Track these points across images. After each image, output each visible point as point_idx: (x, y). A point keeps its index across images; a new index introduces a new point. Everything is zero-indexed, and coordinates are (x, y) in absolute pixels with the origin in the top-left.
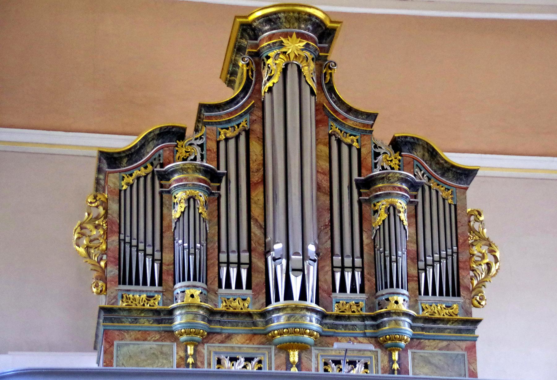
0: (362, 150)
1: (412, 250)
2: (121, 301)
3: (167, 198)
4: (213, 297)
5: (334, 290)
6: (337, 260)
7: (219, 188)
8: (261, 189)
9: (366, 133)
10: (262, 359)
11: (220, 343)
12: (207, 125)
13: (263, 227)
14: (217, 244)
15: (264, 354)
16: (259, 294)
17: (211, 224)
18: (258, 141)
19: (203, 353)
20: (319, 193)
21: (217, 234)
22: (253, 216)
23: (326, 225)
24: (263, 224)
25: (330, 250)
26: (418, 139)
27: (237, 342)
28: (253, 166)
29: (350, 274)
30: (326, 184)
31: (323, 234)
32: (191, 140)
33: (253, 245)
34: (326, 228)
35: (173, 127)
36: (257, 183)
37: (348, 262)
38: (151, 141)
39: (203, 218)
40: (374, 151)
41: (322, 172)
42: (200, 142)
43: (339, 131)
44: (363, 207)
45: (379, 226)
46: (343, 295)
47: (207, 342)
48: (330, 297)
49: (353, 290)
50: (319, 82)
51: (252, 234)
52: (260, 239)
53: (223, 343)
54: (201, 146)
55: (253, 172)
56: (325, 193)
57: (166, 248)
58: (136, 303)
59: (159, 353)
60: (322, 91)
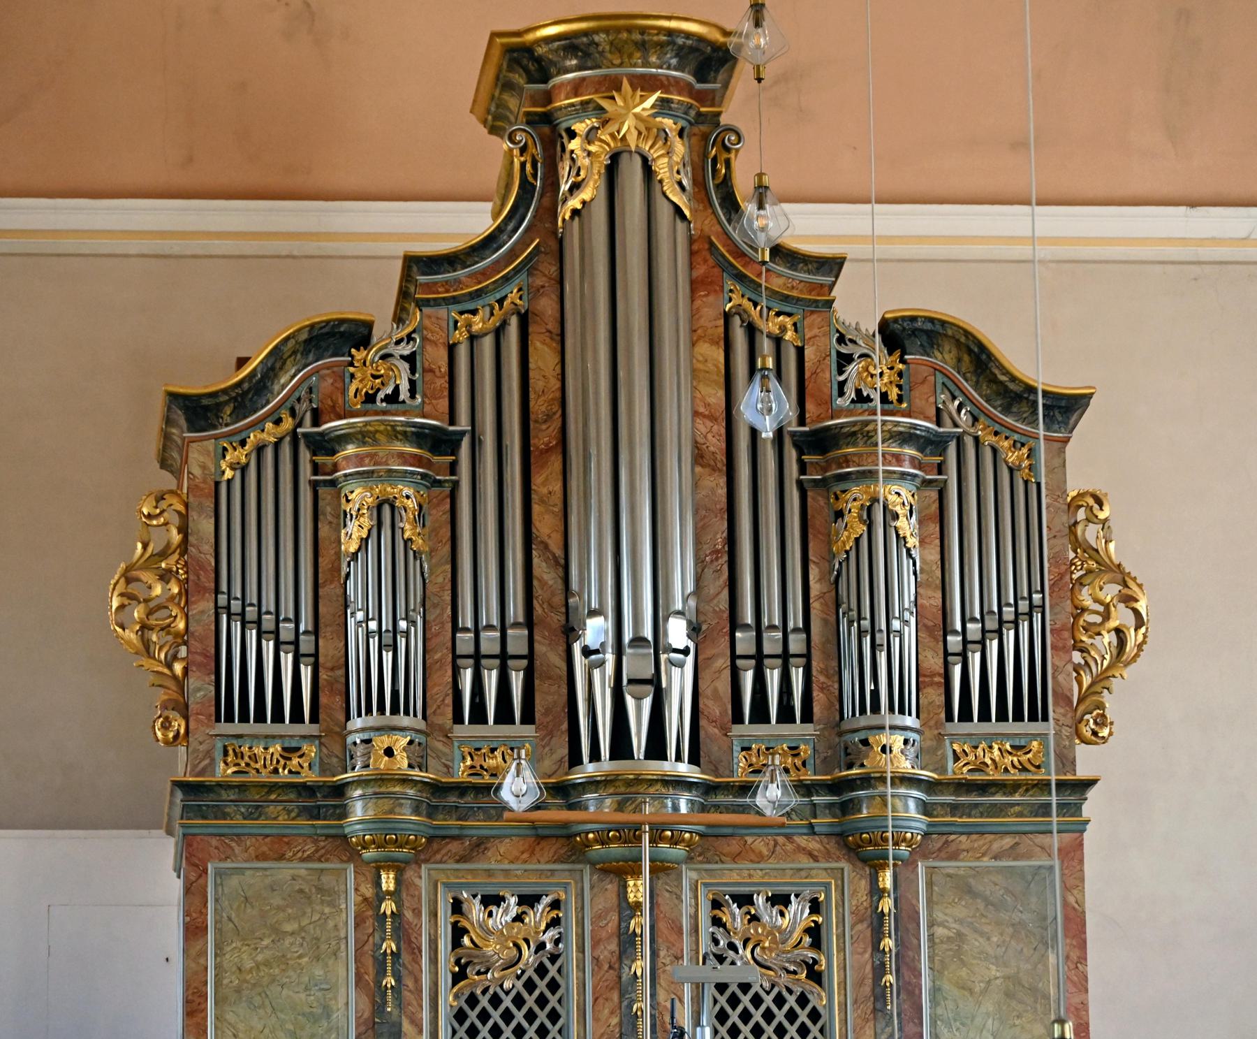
0: (806, 352)
1: (931, 605)
2: (222, 765)
3: (329, 497)
4: (439, 746)
5: (738, 718)
7: (453, 468)
8: (556, 463)
9: (817, 307)
10: (563, 897)
11: (458, 861)
12: (424, 306)
13: (562, 562)
14: (449, 611)
15: (565, 886)
17: (434, 561)
18: (548, 340)
19: (418, 888)
20: (698, 469)
21: (449, 586)
22: (537, 537)
23: (717, 551)
24: (559, 553)
25: (726, 615)
26: (943, 323)
28: (538, 406)
30: (716, 444)
31: (708, 572)
32: (385, 346)
33: (538, 609)
34: (717, 559)
35: (342, 321)
36: (549, 450)
38: (290, 356)
39: (414, 552)
40: (839, 353)
41: (707, 413)
42: (406, 350)
43: (751, 304)
44: (809, 499)
45: (847, 552)
46: (760, 730)
47: (426, 861)
48: (726, 735)
50: (700, 179)
51: (535, 583)
52: (553, 594)
53: (465, 862)
54: (410, 359)
55: (536, 421)
56: (714, 469)
57: (326, 626)
58: (257, 766)
60: (708, 205)
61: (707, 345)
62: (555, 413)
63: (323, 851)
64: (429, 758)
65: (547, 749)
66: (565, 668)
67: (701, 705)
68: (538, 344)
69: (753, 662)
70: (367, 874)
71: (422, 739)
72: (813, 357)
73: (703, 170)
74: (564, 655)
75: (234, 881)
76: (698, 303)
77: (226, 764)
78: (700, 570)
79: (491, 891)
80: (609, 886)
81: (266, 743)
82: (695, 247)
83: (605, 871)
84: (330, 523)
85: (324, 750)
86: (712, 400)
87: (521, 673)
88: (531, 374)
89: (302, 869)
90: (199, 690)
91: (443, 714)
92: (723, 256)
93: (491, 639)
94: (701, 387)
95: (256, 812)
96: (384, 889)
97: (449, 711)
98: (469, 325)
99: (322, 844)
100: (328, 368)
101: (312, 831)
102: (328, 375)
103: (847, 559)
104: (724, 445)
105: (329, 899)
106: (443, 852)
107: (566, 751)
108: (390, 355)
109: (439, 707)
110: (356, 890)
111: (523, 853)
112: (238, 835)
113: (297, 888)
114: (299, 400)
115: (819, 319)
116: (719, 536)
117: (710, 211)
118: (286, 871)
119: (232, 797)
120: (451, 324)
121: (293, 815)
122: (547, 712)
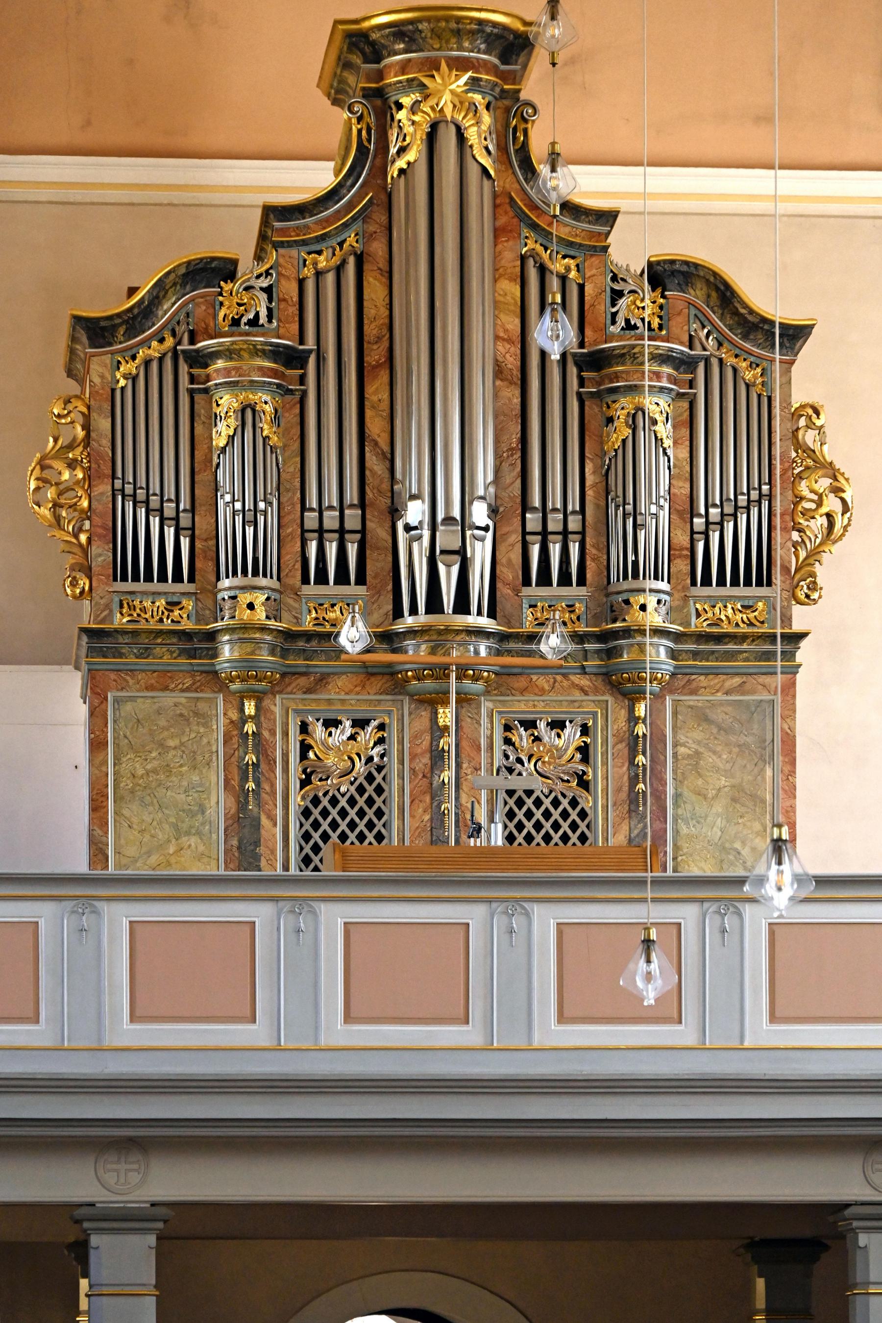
0: (586, 288)
2: (119, 615)
4: (291, 602)
5: (527, 582)
6: (533, 520)
7: (302, 380)
10: (387, 721)
11: (305, 693)
13: (389, 456)
14: (298, 495)
15: (389, 713)
16: (379, 593)
17: (287, 454)
18: (379, 276)
19: (273, 713)
20: (498, 383)
21: (299, 475)
23: (512, 449)
24: (386, 448)
25: (519, 500)
27: (337, 690)
28: (370, 330)
29: (558, 546)
30: (512, 362)
32: (248, 280)
33: (369, 494)
34: (512, 455)
36: (378, 366)
37: (555, 523)
40: (612, 290)
44: (587, 408)
45: (616, 451)
46: (544, 591)
47: (280, 692)
49: (565, 580)
51: (367, 473)
52: (382, 482)
53: (311, 693)
54: (268, 290)
55: (369, 343)
56: (511, 383)
58: (147, 616)
59: (191, 714)
60: (509, 166)
61: (507, 282)
62: (384, 336)
63: (199, 684)
64: (283, 612)
65: (375, 606)
66: (390, 541)
67: (498, 572)
68: (371, 279)
69: (539, 537)
70: (234, 702)
71: (277, 596)
72: (591, 292)
73: (506, 137)
74: (390, 530)
75: (128, 707)
76: (500, 247)
77: (122, 614)
78: (498, 463)
79: (331, 716)
80: (423, 713)
82: (498, 201)
83: (421, 702)
84: (204, 423)
85: (200, 604)
86: (509, 327)
87: (356, 545)
88: (365, 304)
89: (182, 698)
90: (100, 555)
91: (294, 576)
92: (521, 209)
93: (333, 518)
94: (502, 316)
95: (146, 652)
96: (247, 714)
97: (299, 574)
98: (315, 264)
99: (198, 678)
100: (202, 297)
101: (190, 668)
102: (201, 303)
103: (616, 455)
104: (519, 363)
105: (203, 721)
106: (293, 685)
107: (391, 607)
108: (251, 287)
109: (290, 571)
110: (225, 714)
111: (356, 686)
112: (131, 671)
113: (178, 712)
114: (178, 323)
115: (597, 261)
116: (514, 436)
117: (510, 171)
118: (168, 699)
119: (126, 641)
120: (301, 262)
121: (175, 655)
122: (376, 577)
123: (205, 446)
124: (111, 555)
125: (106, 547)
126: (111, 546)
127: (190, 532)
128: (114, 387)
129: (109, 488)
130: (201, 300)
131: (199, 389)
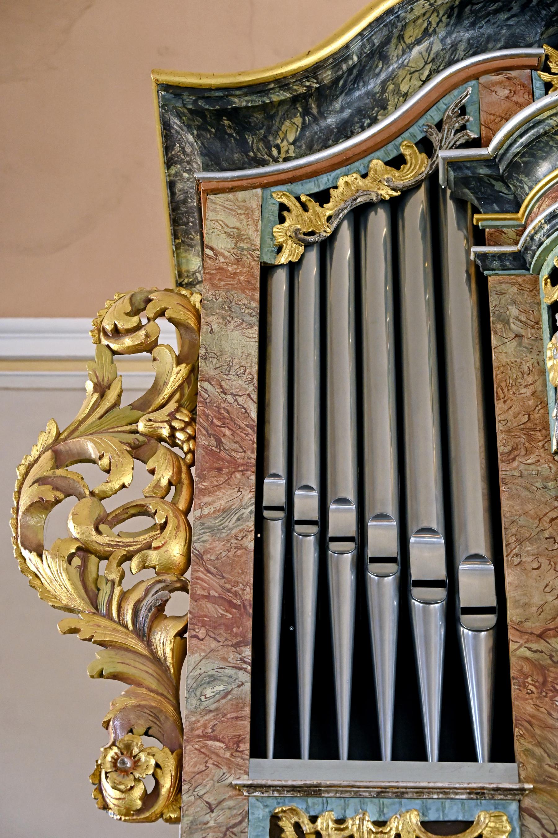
3: (514, 289)
57: (520, 542)
81: (381, 812)
90: (213, 680)
100: (498, 71)
102: (500, 83)
114: (439, 126)
123: (528, 392)
124: (246, 678)
125: (232, 656)
126: (248, 652)
127: (491, 619)
128: (268, 259)
129: (249, 496)
130: (494, 78)
131: (501, 256)
